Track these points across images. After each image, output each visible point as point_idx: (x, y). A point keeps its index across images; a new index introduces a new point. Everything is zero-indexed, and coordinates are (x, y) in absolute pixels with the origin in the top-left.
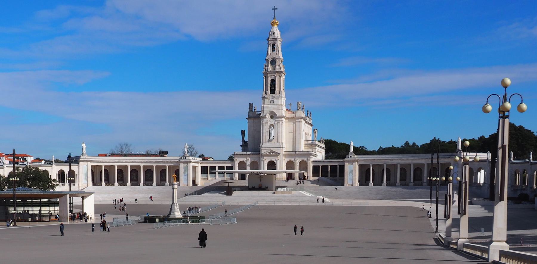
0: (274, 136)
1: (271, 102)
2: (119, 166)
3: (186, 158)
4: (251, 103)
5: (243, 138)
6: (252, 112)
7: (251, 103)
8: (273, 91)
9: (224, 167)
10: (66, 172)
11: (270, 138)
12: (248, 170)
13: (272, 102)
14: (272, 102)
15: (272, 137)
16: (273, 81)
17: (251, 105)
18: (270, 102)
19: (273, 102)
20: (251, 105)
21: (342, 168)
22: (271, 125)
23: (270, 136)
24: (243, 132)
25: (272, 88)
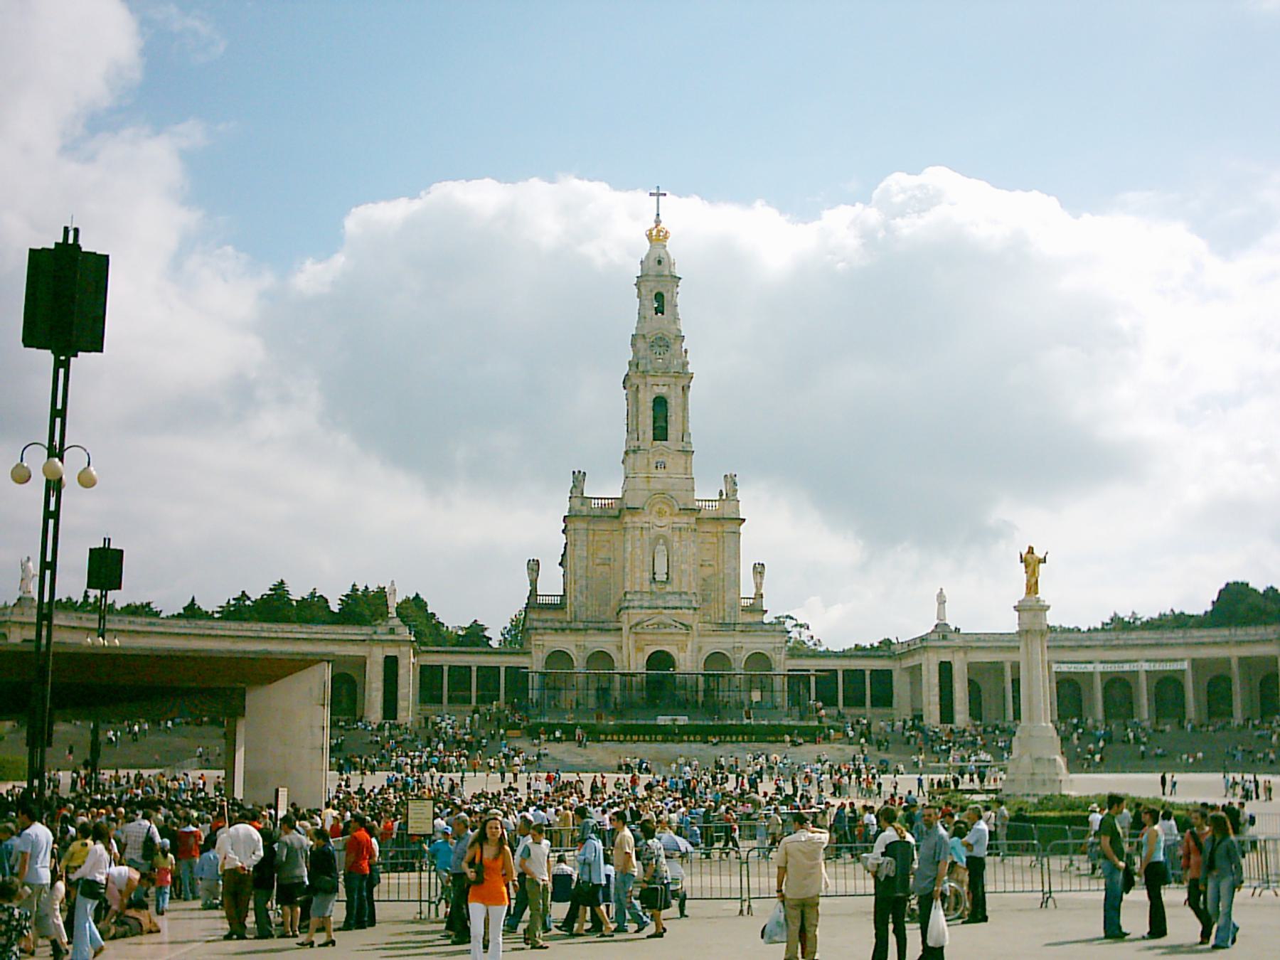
0: (667, 574)
1: (657, 467)
5: (534, 584)
8: (660, 433)
13: (661, 465)
15: (661, 576)
16: (660, 404)
17: (579, 478)
20: (579, 478)
22: (657, 538)
23: (654, 574)
25: (657, 425)
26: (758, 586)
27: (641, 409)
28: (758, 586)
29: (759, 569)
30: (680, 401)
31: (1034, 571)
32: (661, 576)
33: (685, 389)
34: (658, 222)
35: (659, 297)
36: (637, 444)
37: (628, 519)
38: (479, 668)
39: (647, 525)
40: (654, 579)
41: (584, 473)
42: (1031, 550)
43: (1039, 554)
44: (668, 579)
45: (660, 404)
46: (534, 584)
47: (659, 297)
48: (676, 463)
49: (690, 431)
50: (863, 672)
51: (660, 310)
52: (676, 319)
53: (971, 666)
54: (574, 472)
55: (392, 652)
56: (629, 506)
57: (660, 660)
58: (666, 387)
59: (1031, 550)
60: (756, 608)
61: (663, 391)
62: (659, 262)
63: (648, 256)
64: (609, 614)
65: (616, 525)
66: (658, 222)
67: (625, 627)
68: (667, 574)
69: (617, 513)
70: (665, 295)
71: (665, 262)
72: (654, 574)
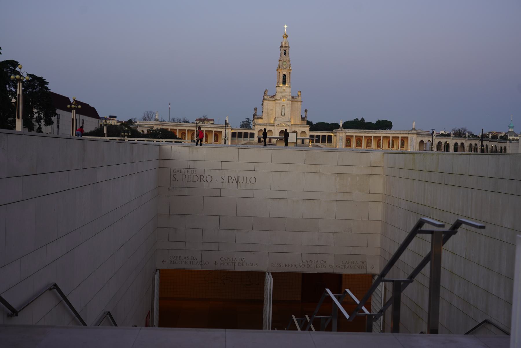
2: (245, 133)
9: (314, 135)
10: (459, 144)
11: (282, 115)
12: (315, 138)
15: (283, 114)
21: (330, 138)
23: (282, 114)
27: (280, 77)
30: (289, 75)
32: (283, 114)
35: (285, 51)
38: (244, 133)
40: (282, 115)
44: (284, 115)
45: (284, 75)
50: (326, 136)
53: (346, 136)
58: (286, 73)
62: (285, 43)
64: (272, 122)
68: (285, 114)
71: (287, 44)
72: (282, 114)
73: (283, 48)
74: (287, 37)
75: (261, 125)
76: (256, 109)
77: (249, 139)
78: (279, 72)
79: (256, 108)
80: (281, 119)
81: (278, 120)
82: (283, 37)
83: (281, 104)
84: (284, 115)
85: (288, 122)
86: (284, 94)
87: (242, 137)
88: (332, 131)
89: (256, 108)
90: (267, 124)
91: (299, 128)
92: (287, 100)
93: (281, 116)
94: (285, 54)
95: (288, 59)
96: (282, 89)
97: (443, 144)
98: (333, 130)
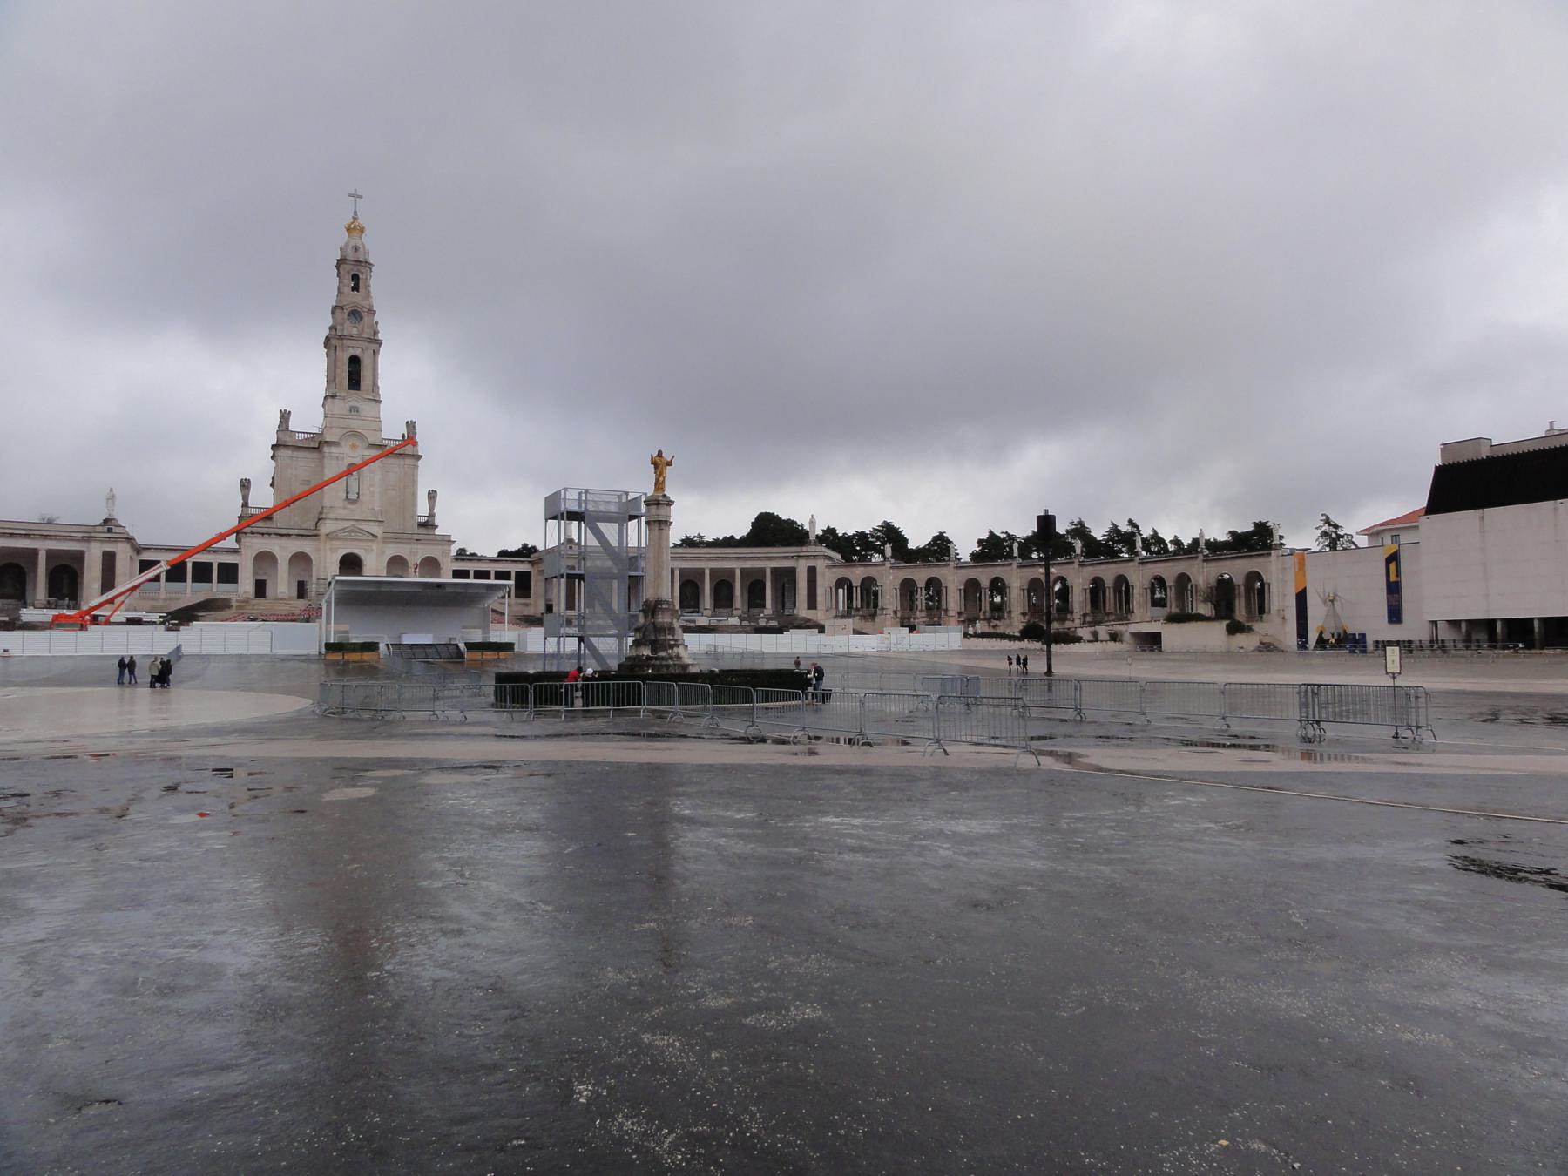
0: (358, 494)
3: (110, 530)
4: (285, 411)
5: (245, 498)
6: (289, 433)
7: (285, 411)
8: (355, 382)
11: (347, 497)
13: (354, 409)
14: (354, 410)
15: (353, 496)
16: (355, 361)
17: (285, 417)
18: (348, 409)
19: (357, 412)
23: (347, 493)
24: (245, 485)
26: (432, 508)
27: (339, 364)
28: (432, 508)
29: (432, 496)
31: (661, 474)
33: (375, 353)
34: (355, 219)
35: (355, 278)
36: (335, 391)
37: (326, 449)
39: (342, 455)
40: (347, 497)
41: (290, 412)
42: (660, 454)
43: (667, 457)
44: (358, 497)
45: (355, 361)
46: (245, 498)
47: (355, 278)
48: (366, 408)
49: (379, 385)
51: (356, 288)
52: (368, 295)
54: (281, 411)
55: (109, 547)
56: (327, 440)
57: (351, 563)
59: (660, 454)
60: (428, 525)
61: (358, 352)
63: (347, 245)
64: (311, 524)
65: (315, 455)
66: (355, 219)
67: (322, 537)
68: (358, 494)
69: (317, 445)
70: (360, 276)
73: (348, 267)
74: (362, 230)
75: (263, 534)
76: (245, 485)
77: (216, 589)
78: (336, 348)
79: (248, 481)
80: (343, 513)
81: (332, 515)
82: (349, 230)
83: (343, 458)
84: (358, 497)
85: (372, 523)
86: (355, 424)
87: (185, 581)
88: (529, 557)
89: (248, 481)
90: (291, 532)
91: (415, 546)
92: (365, 445)
93: (346, 502)
94: (356, 288)
95: (365, 303)
96: (348, 406)
97: (921, 584)
98: (532, 556)
